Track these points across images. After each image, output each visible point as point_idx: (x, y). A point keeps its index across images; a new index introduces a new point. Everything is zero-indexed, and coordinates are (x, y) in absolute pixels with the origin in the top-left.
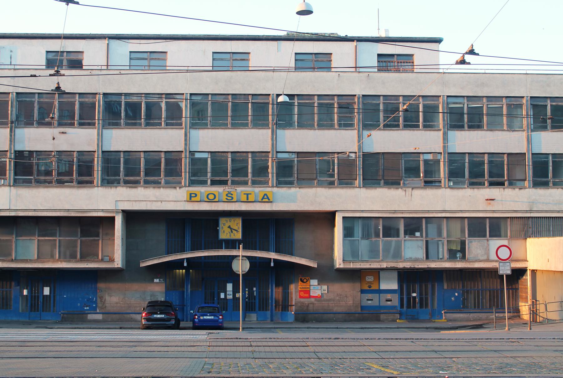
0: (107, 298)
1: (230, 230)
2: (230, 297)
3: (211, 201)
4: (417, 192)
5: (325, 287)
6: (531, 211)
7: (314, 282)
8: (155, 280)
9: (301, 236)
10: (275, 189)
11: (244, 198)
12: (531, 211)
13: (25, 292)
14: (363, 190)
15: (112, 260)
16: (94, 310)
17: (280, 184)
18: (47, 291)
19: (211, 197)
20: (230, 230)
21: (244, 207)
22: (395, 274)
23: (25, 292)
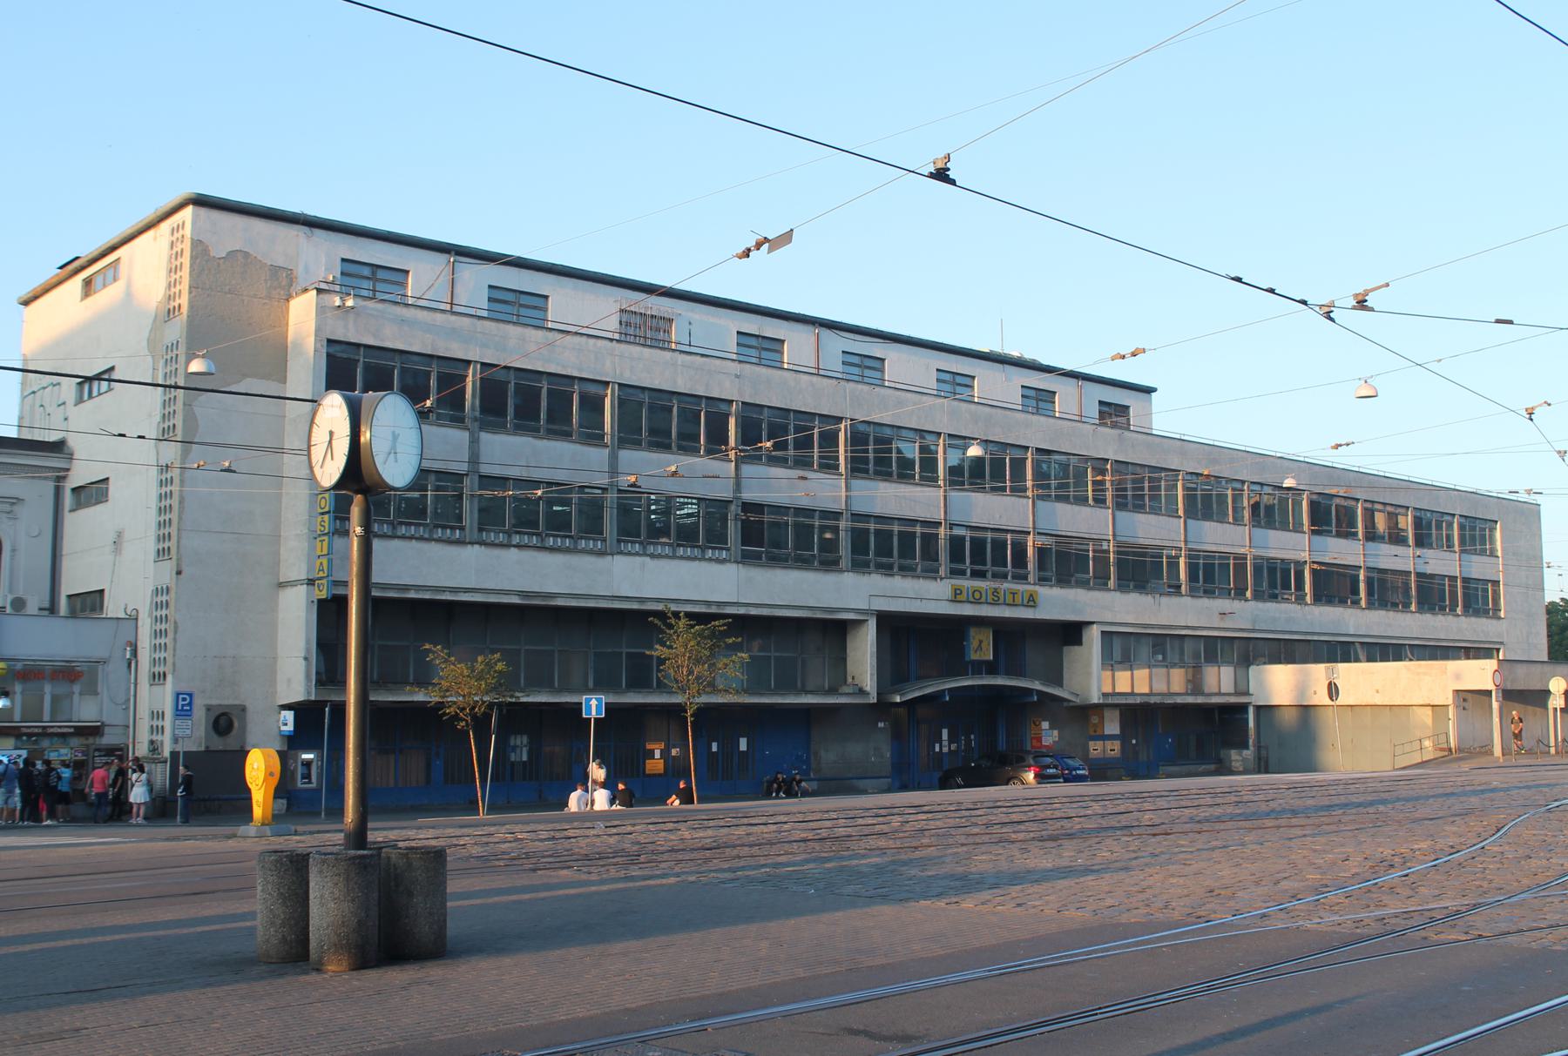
0: (823, 753)
1: (981, 647)
2: (945, 750)
3: (977, 602)
4: (1164, 600)
5: (1056, 733)
6: (1253, 631)
7: (1045, 725)
8: (881, 725)
9: (1033, 655)
10: (1037, 588)
11: (1009, 599)
12: (1253, 631)
13: (714, 747)
14: (1118, 594)
15: (862, 692)
16: (806, 775)
17: (1043, 580)
18: (743, 744)
19: (977, 595)
20: (981, 647)
21: (1007, 613)
22: (1117, 713)
23: (714, 747)
